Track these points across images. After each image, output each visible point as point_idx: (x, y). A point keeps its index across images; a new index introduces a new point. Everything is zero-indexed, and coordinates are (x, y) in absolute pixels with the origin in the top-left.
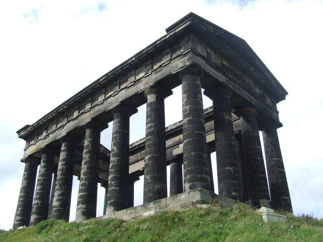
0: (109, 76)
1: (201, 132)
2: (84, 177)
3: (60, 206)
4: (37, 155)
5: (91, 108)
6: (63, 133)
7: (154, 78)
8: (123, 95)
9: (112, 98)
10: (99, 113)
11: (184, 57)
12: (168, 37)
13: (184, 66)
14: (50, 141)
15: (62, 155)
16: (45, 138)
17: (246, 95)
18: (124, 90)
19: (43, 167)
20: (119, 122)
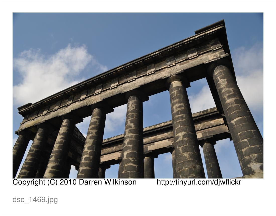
2: (89, 151)
5: (101, 92)
7: (179, 68)
9: (127, 84)
12: (197, 37)
18: (143, 78)
20: (136, 103)
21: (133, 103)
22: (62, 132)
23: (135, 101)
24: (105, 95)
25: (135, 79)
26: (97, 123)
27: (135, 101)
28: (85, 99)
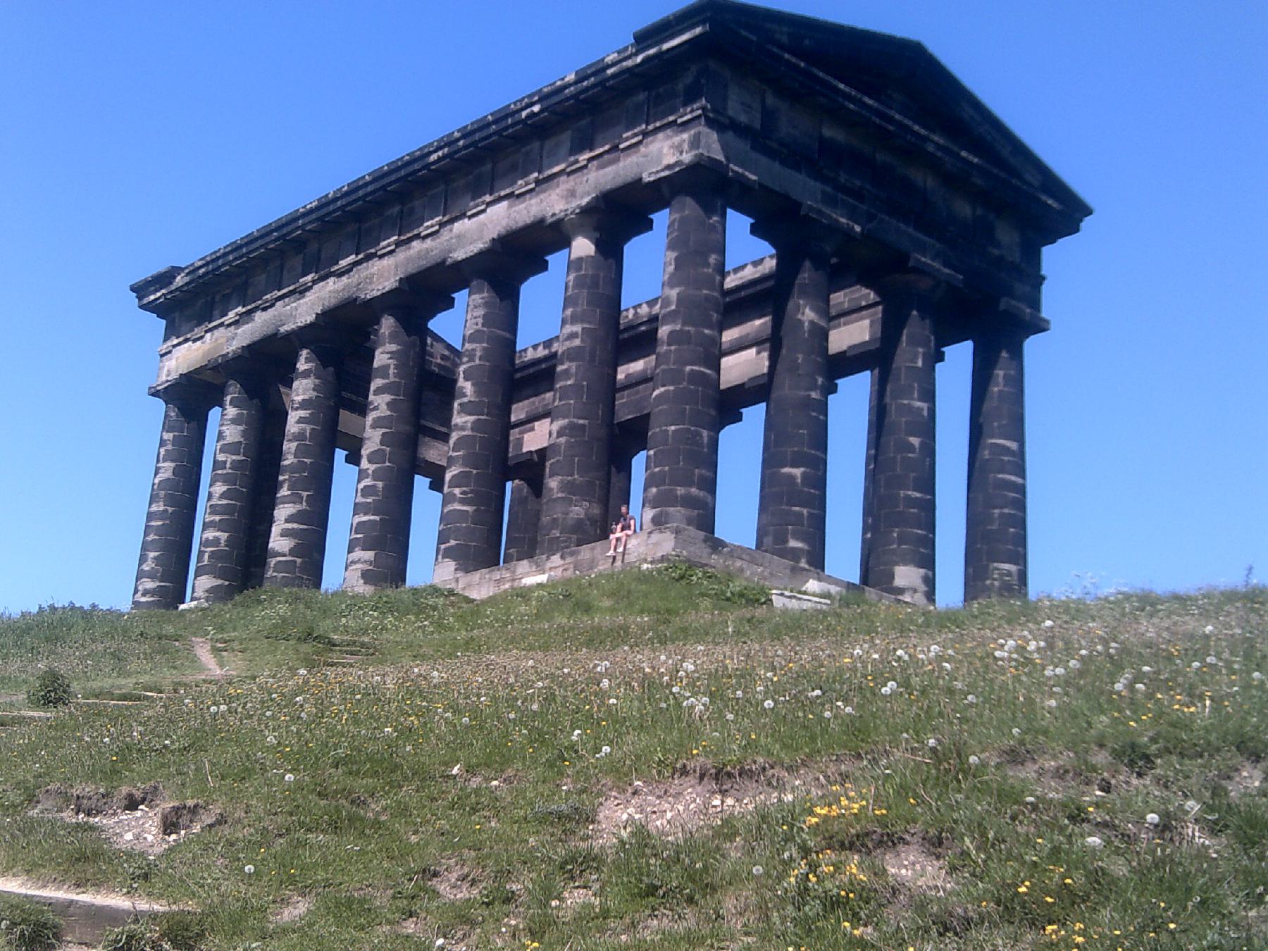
0: (460, 150)
1: (702, 369)
2: (372, 467)
3: (292, 552)
4: (208, 376)
10: (424, 263)
11: (682, 132)
13: (677, 163)
14: (256, 337)
15: (302, 390)
16: (236, 323)
18: (505, 204)
19: (234, 421)
20: (486, 304)
21: (476, 307)
22: (299, 398)
23: (483, 298)
24: (409, 259)
25: (483, 207)
26: (391, 371)
27: (483, 298)
28: (351, 270)
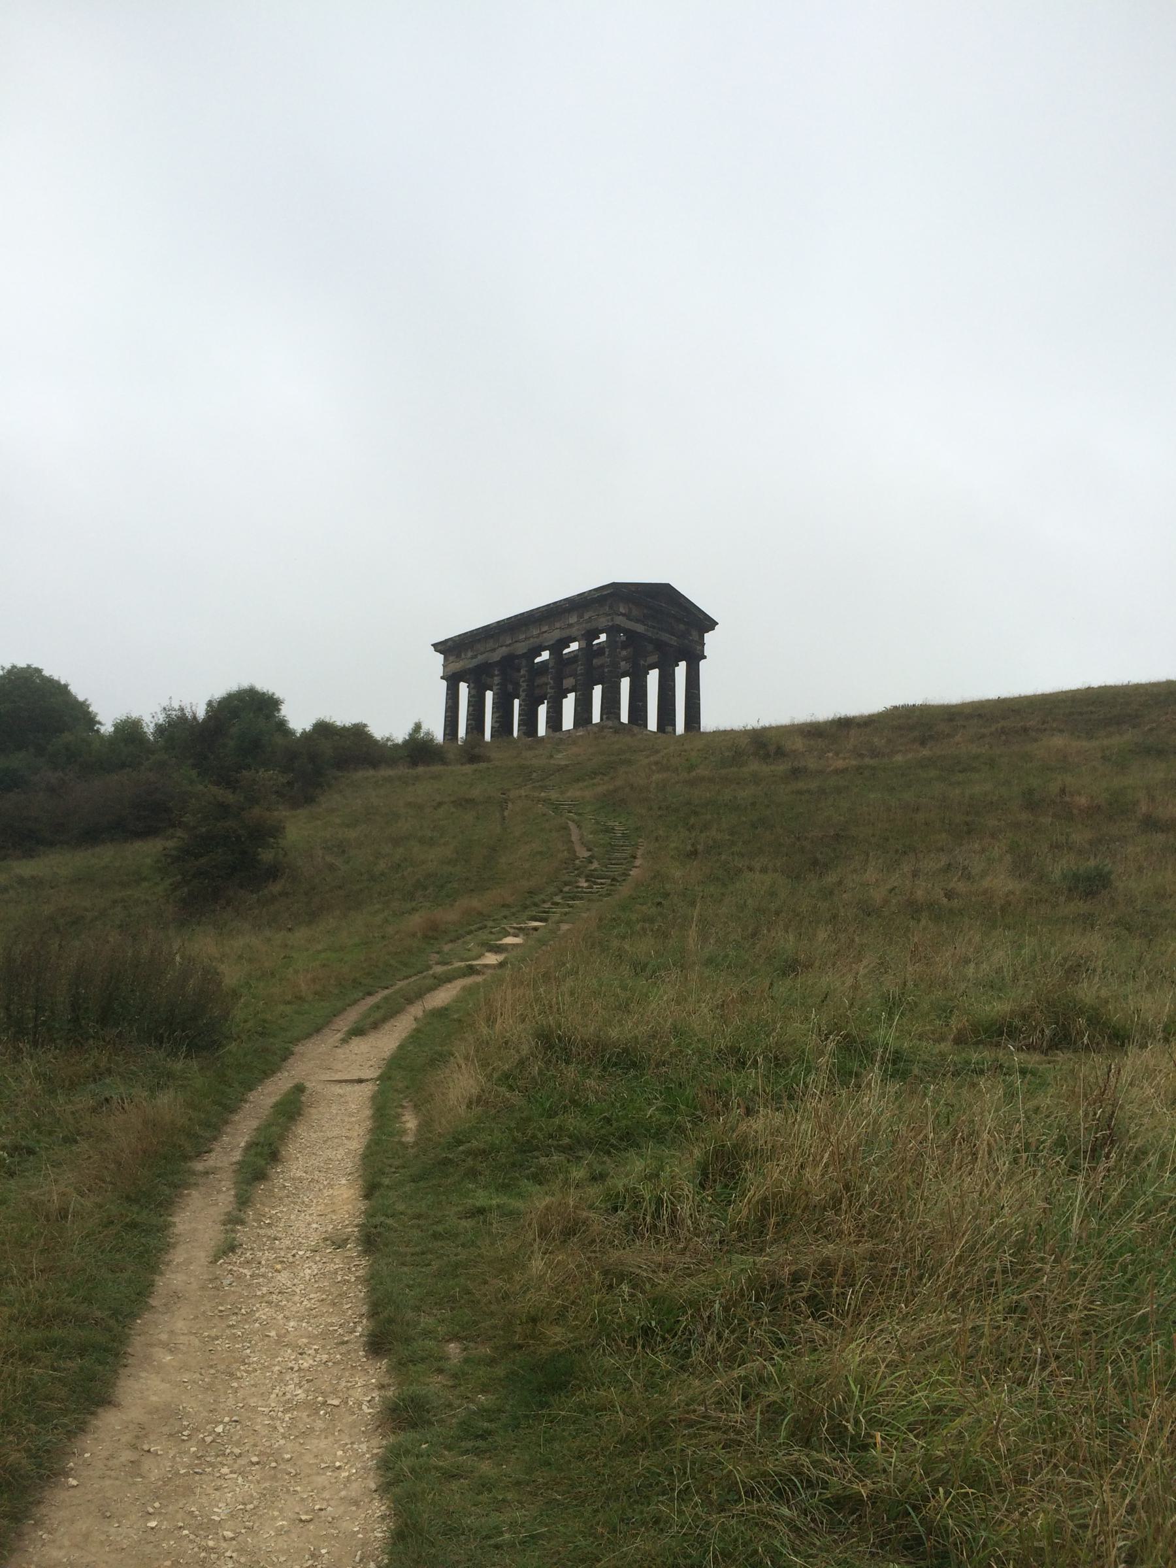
6: (496, 656)
8: (557, 635)
16: (472, 658)
17: (665, 637)
